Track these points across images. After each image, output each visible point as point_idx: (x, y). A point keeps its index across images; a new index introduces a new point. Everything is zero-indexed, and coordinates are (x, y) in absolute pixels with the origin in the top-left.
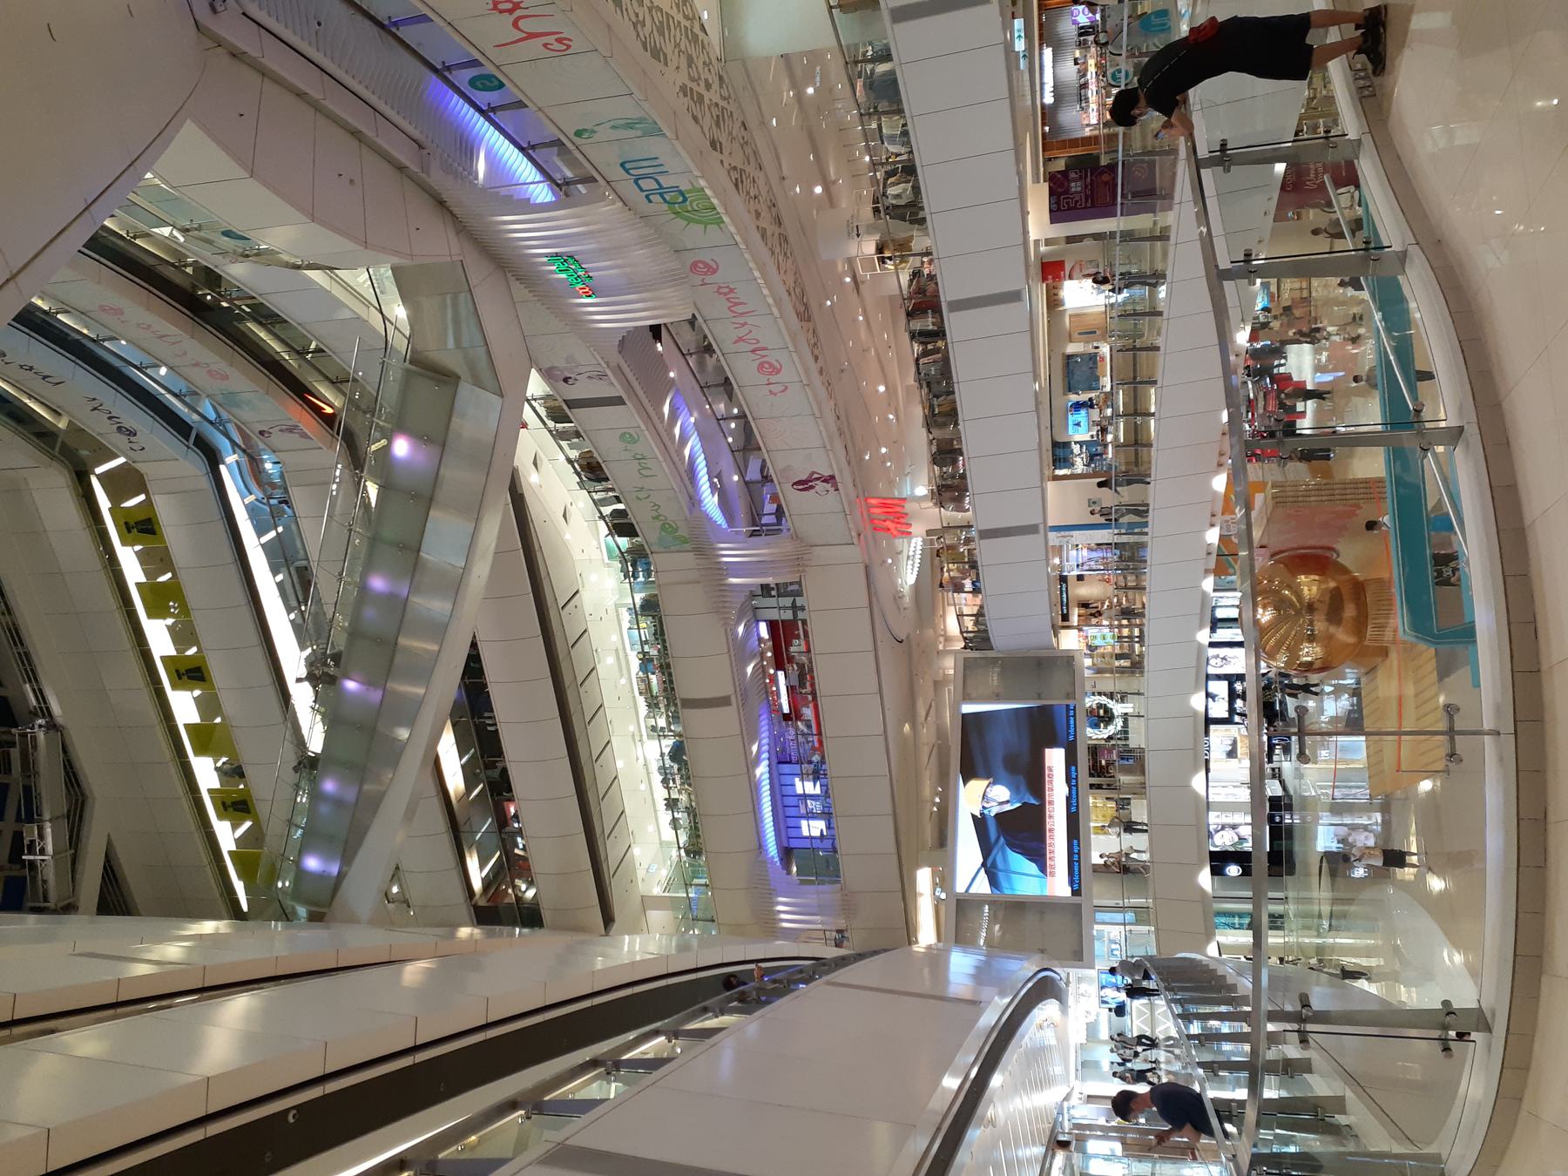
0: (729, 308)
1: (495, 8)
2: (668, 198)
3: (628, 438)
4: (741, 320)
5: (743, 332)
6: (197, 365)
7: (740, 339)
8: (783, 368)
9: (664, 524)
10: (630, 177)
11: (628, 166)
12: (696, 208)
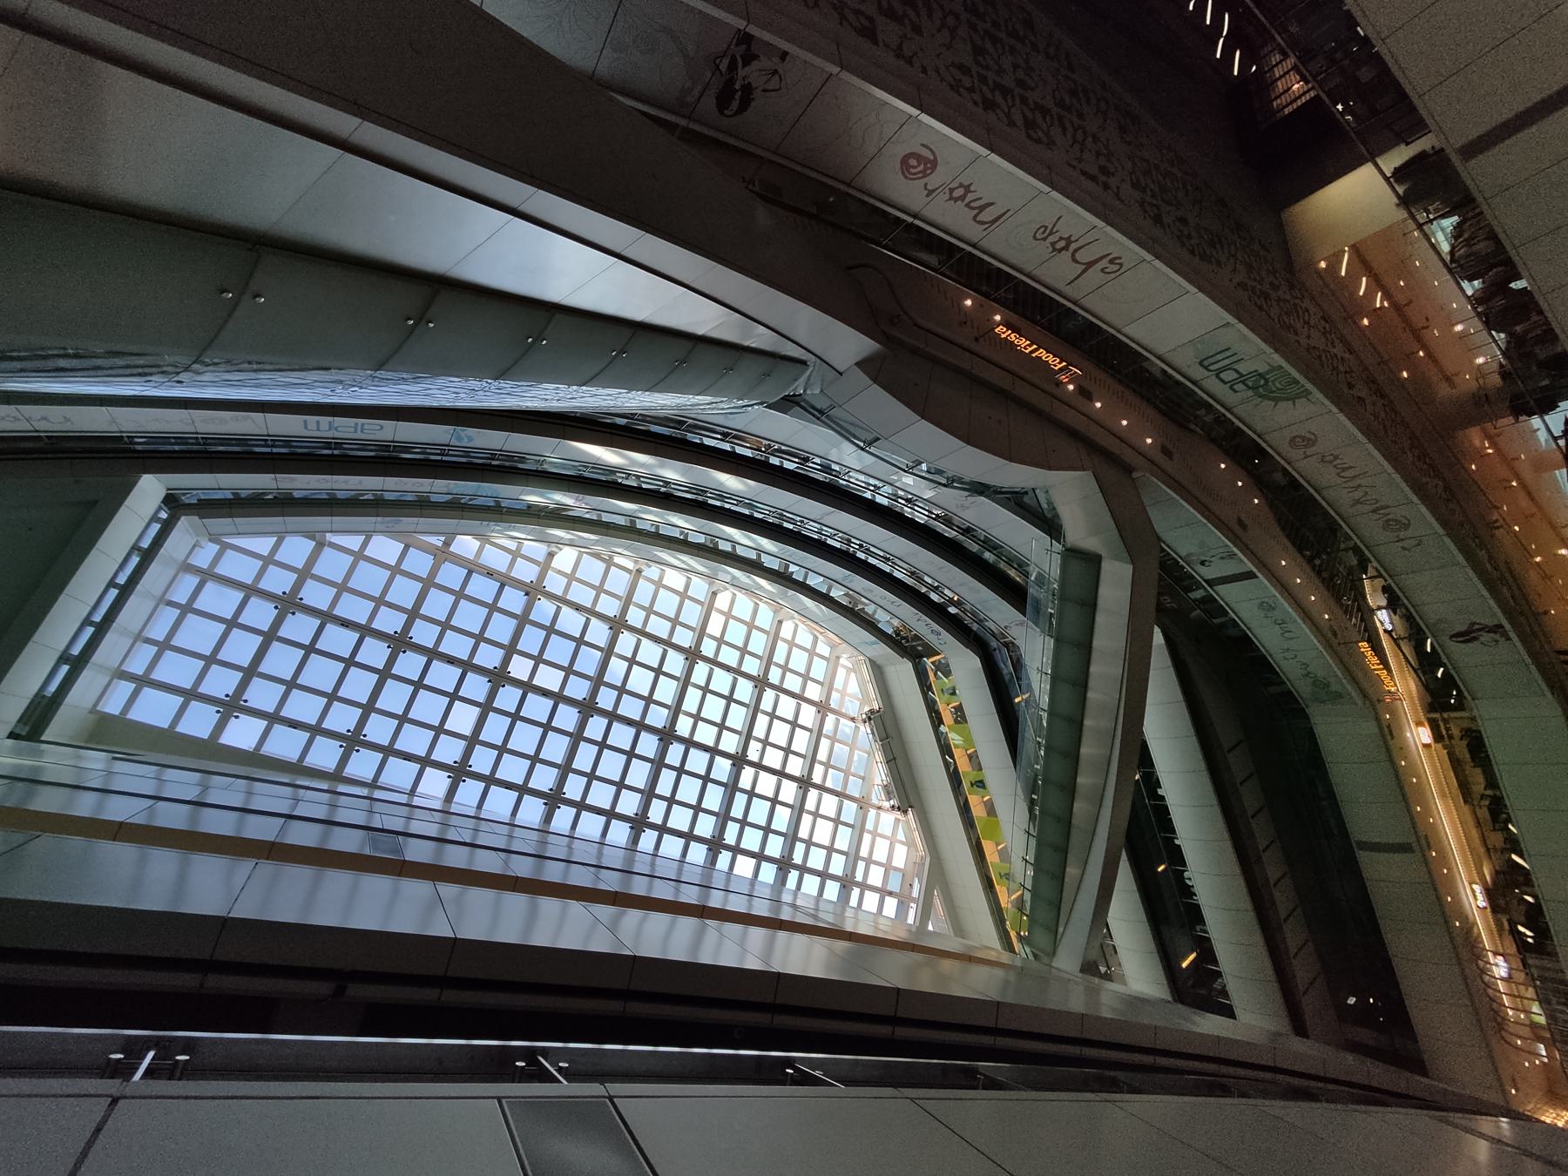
0: (1338, 474)
1: (1054, 250)
2: (1250, 384)
3: (1267, 607)
5: (1357, 495)
6: (961, 585)
7: (1358, 502)
8: (1412, 521)
9: (1314, 681)
10: (1211, 373)
11: (1206, 363)
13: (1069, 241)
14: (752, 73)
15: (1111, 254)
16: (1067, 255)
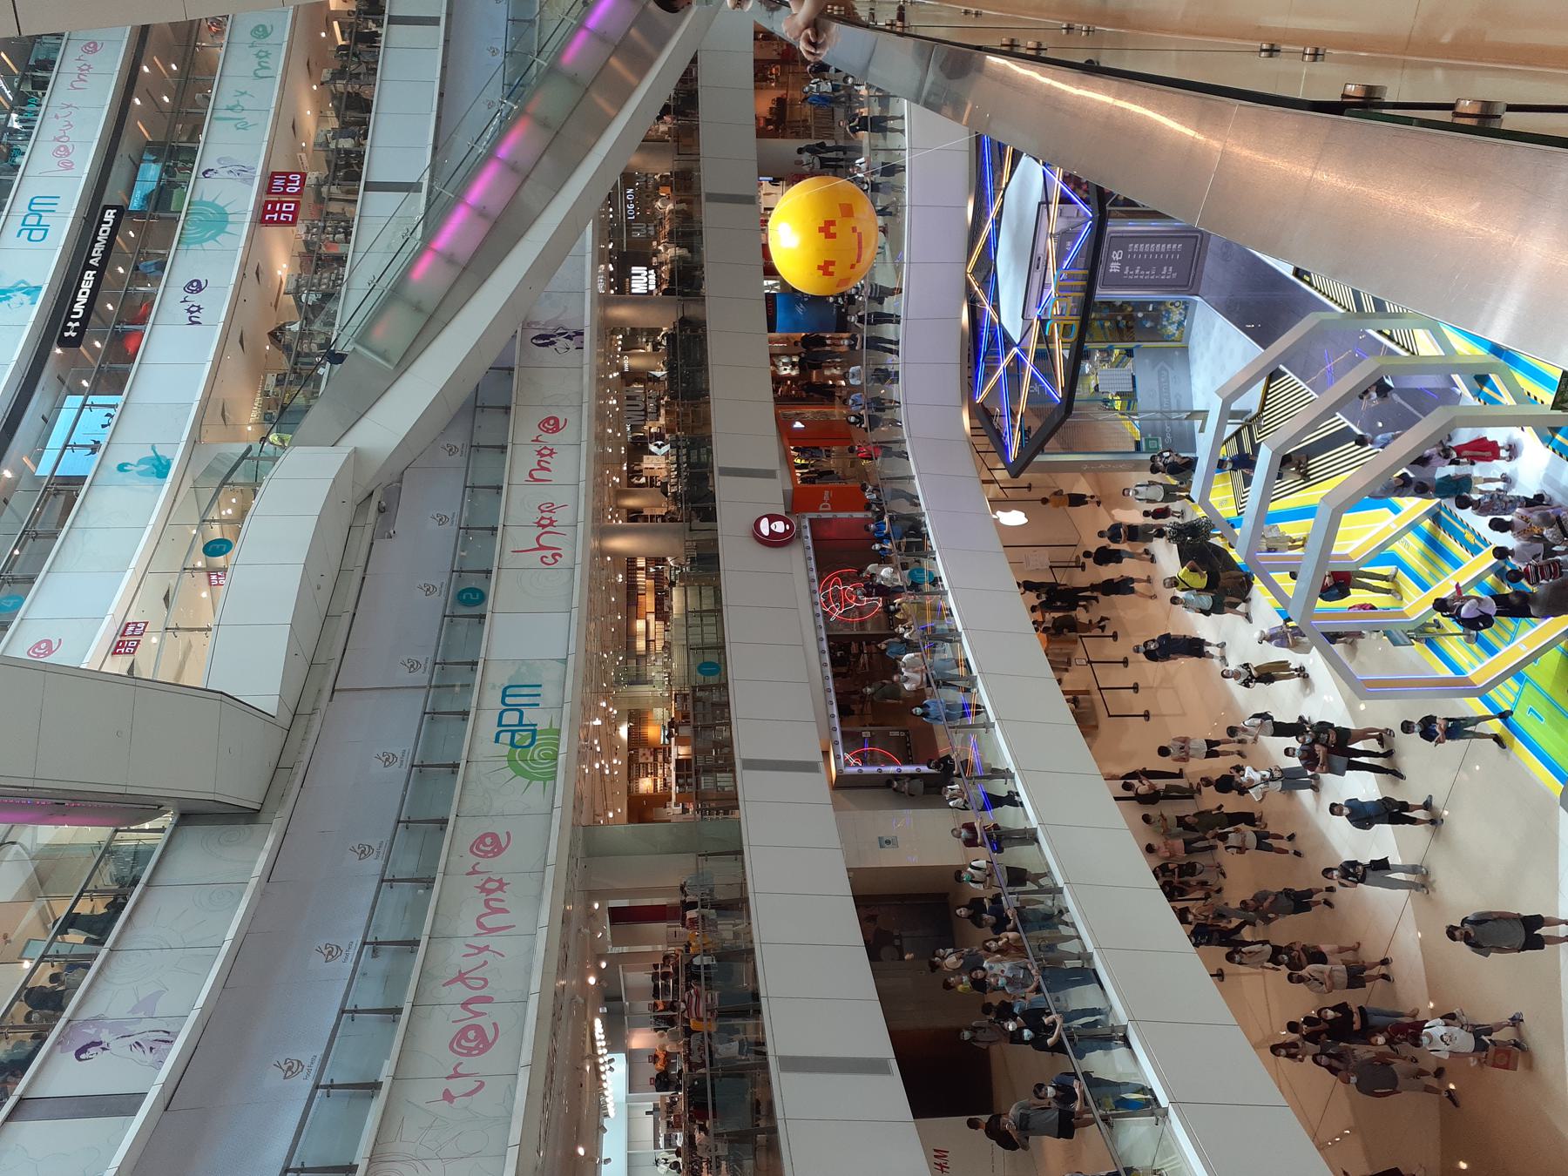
4: (480, 942)
7: (461, 977)
12: (536, 757)
13: (552, 523)
14: (561, 342)
15: (560, 549)
16: (540, 530)
